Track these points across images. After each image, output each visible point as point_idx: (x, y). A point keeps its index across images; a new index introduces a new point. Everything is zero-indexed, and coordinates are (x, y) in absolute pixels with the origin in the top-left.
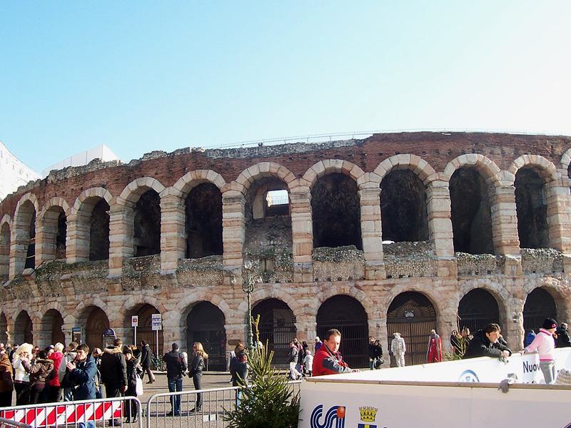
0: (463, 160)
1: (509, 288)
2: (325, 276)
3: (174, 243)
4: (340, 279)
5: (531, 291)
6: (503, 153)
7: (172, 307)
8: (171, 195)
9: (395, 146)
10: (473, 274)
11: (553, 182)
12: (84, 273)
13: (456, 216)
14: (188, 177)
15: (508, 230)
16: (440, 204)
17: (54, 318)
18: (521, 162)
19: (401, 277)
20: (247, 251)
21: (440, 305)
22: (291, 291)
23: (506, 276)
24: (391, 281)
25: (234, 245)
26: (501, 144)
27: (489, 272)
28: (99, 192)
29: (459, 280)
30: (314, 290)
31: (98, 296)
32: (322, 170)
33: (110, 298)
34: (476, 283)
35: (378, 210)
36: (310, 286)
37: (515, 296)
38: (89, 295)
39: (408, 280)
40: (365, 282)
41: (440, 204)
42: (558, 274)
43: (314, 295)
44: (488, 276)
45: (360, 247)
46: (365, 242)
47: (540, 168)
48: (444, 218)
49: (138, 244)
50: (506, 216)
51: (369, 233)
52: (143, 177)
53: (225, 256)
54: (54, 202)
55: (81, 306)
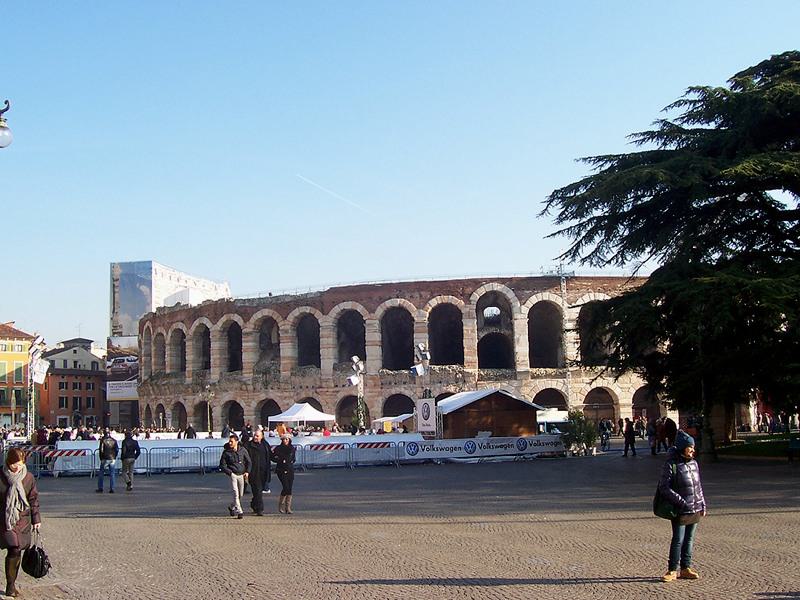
0: (389, 303)
3: (218, 362)
6: (421, 296)
8: (216, 328)
12: (173, 380)
16: (373, 336)
17: (161, 408)
24: (337, 389)
26: (419, 290)
27: (405, 383)
28: (180, 326)
30: (292, 394)
33: (187, 397)
34: (394, 391)
41: (373, 336)
43: (292, 397)
45: (319, 366)
49: (206, 359)
50: (422, 342)
55: (173, 403)
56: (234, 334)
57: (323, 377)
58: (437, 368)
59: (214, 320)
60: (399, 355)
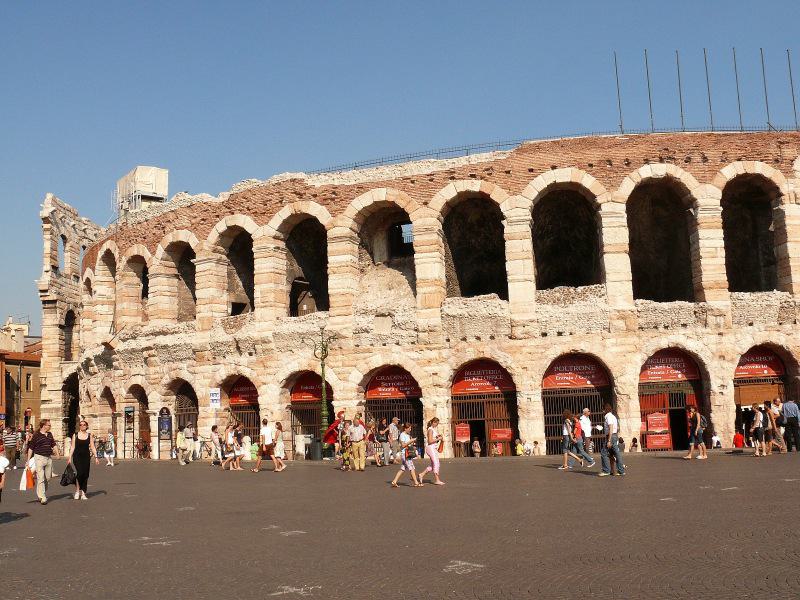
0: (647, 171)
1: (713, 348)
2: (460, 335)
3: (271, 297)
4: (478, 338)
5: (745, 352)
6: (705, 159)
7: (269, 379)
8: (265, 234)
9: (552, 159)
10: (661, 329)
11: (783, 198)
13: (636, 250)
14: (285, 213)
15: (712, 267)
16: (615, 232)
18: (730, 172)
19: (560, 334)
20: (360, 306)
21: (615, 373)
22: (414, 355)
23: (708, 330)
25: (344, 298)
27: (684, 325)
29: (639, 337)
31: (183, 365)
32: (455, 194)
33: (198, 369)
34: (665, 342)
35: (528, 244)
36: (439, 349)
37: (722, 357)
38: (174, 365)
39: (569, 338)
40: (512, 342)
41: (615, 232)
42: (788, 326)
43: (444, 360)
44: (682, 331)
45: (504, 296)
46: (513, 288)
47: (759, 177)
48: (619, 252)
51: (515, 277)
52: (233, 214)
53: (332, 311)
54: (135, 250)
55: (167, 380)
56: (306, 241)
57: (516, 317)
58: (747, 295)
59: (262, 215)
60: (665, 273)
